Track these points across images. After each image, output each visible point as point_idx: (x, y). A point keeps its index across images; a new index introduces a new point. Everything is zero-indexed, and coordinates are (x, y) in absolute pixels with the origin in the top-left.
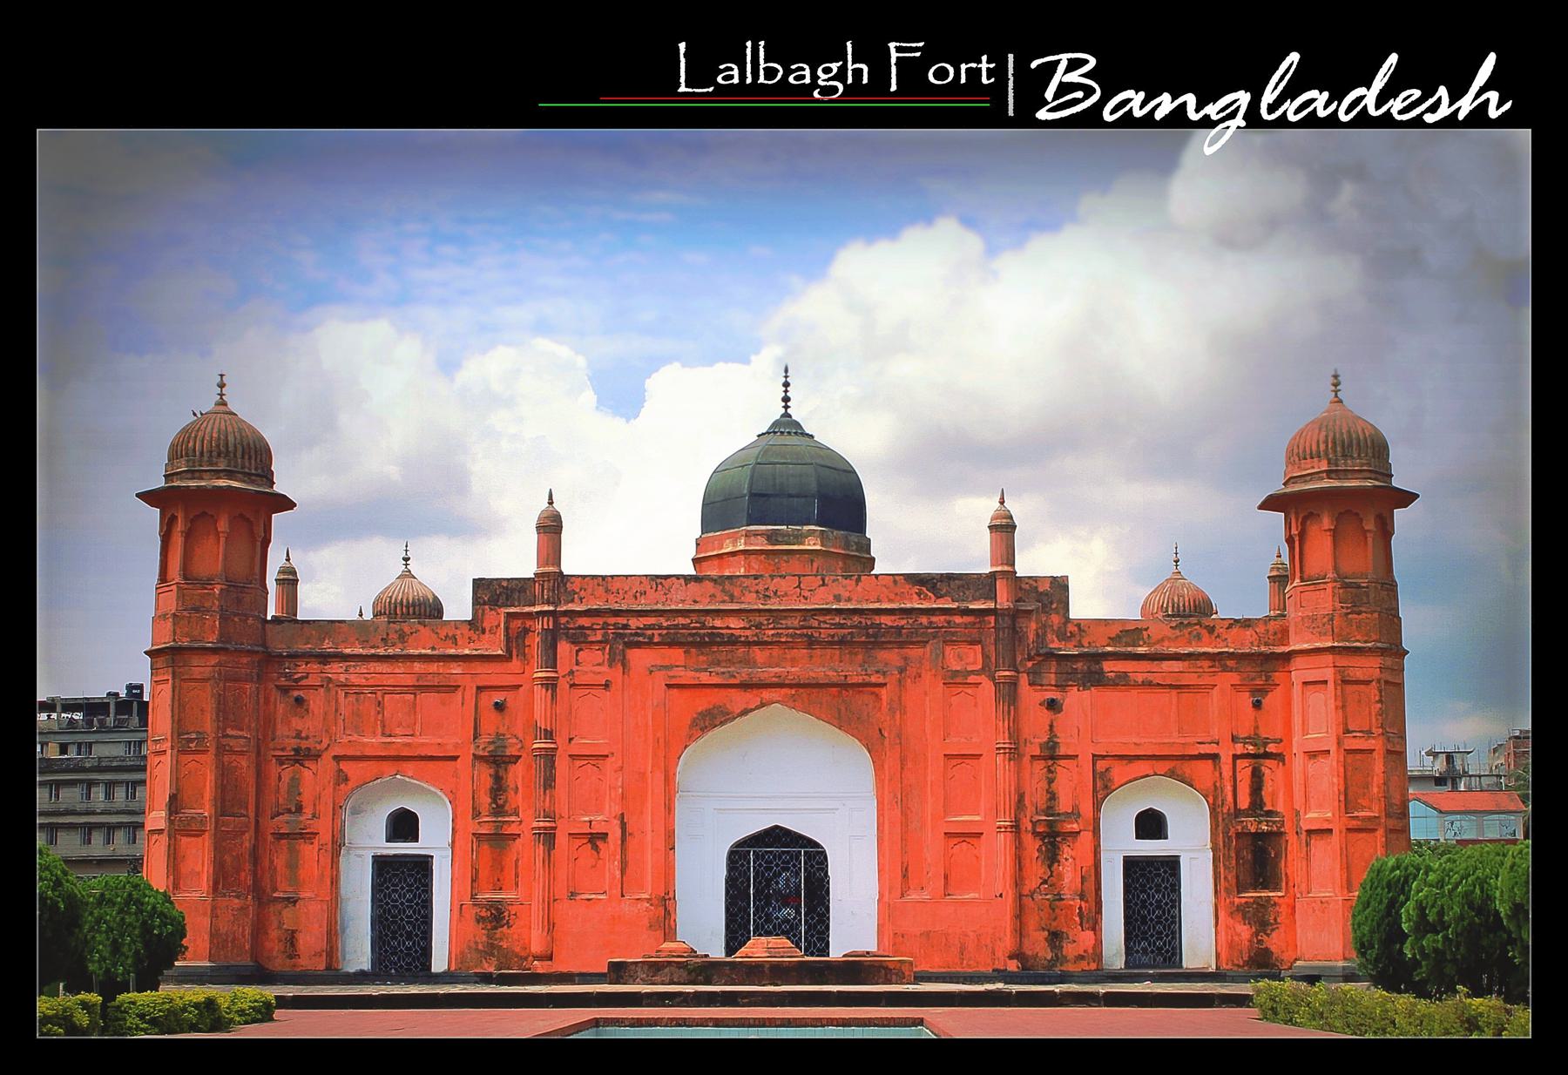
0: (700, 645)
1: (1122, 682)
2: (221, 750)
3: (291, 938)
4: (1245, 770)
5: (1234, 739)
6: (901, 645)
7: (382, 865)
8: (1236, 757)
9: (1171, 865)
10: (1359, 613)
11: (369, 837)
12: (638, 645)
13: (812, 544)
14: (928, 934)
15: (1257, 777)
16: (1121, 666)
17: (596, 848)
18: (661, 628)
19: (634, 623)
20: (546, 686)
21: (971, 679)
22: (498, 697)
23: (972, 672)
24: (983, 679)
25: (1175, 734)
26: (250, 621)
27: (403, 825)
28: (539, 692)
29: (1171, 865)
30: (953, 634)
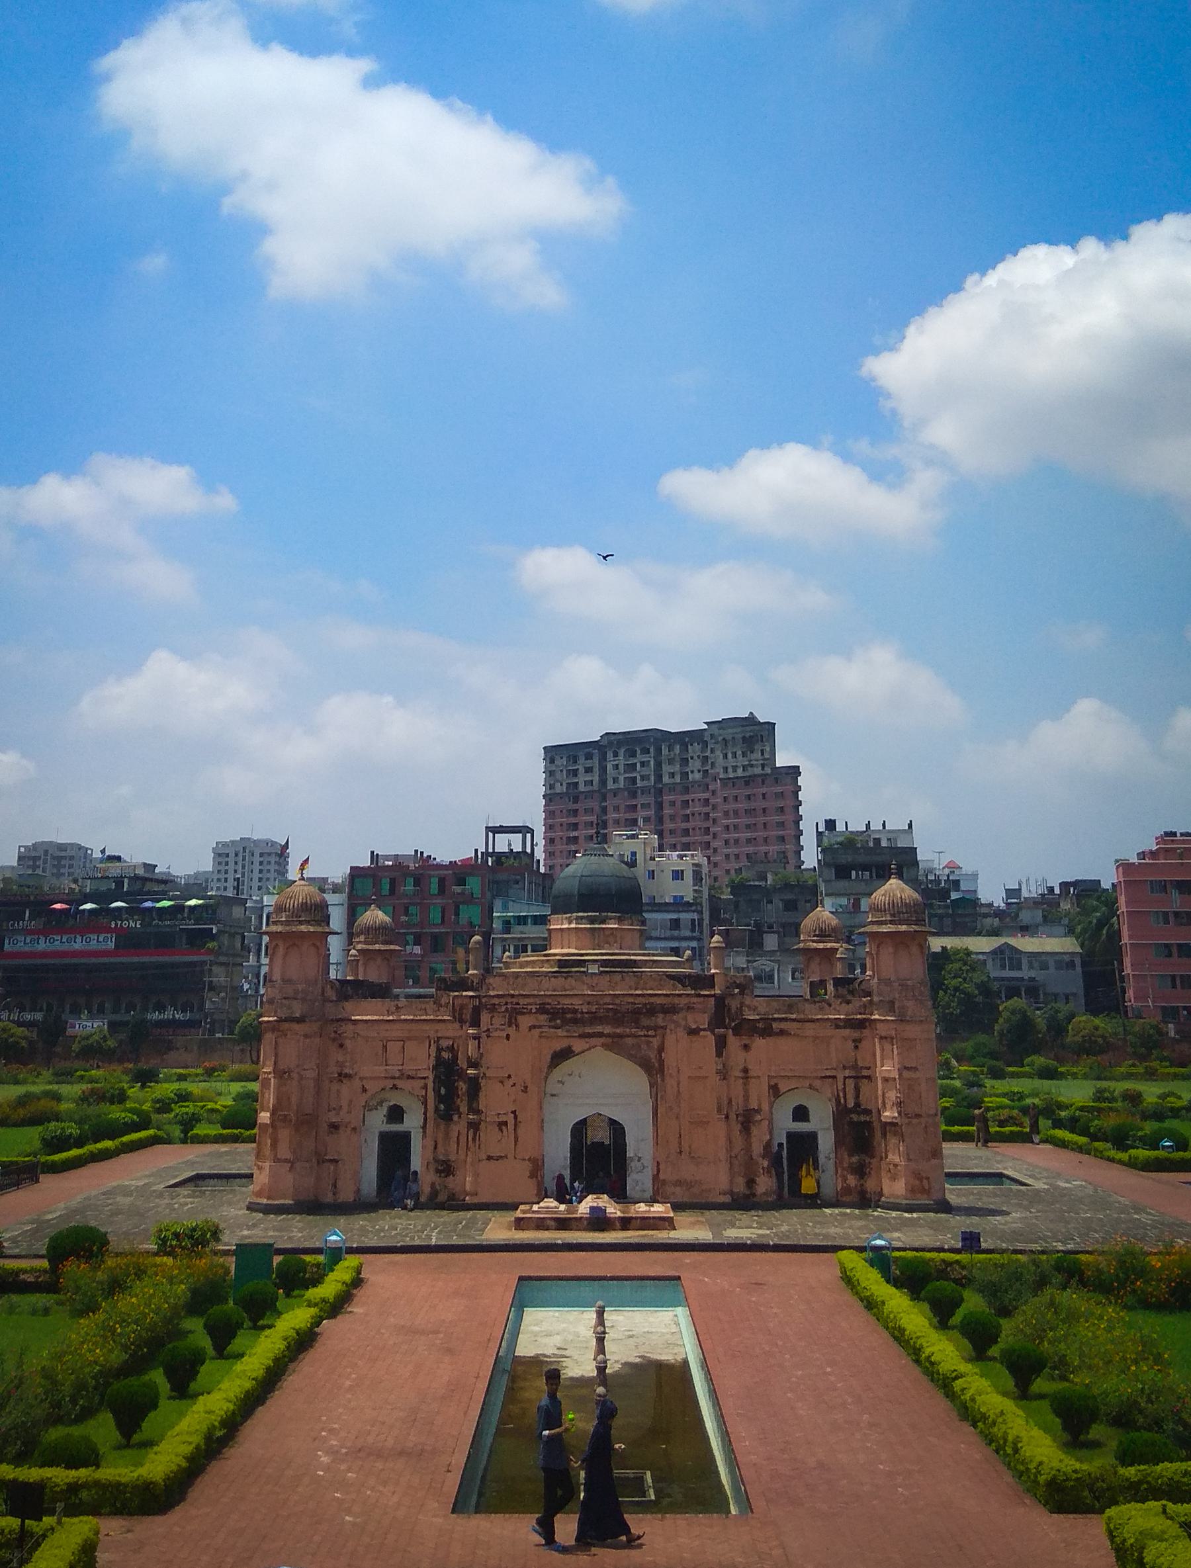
1: (782, 1033)
4: (851, 1084)
5: (845, 1068)
7: (384, 1137)
8: (845, 1078)
9: (813, 1136)
11: (377, 1122)
12: (524, 1013)
15: (857, 1089)
16: (783, 1025)
19: (521, 1001)
20: (475, 1038)
21: (702, 1033)
23: (704, 1030)
27: (396, 1114)
29: (813, 1136)
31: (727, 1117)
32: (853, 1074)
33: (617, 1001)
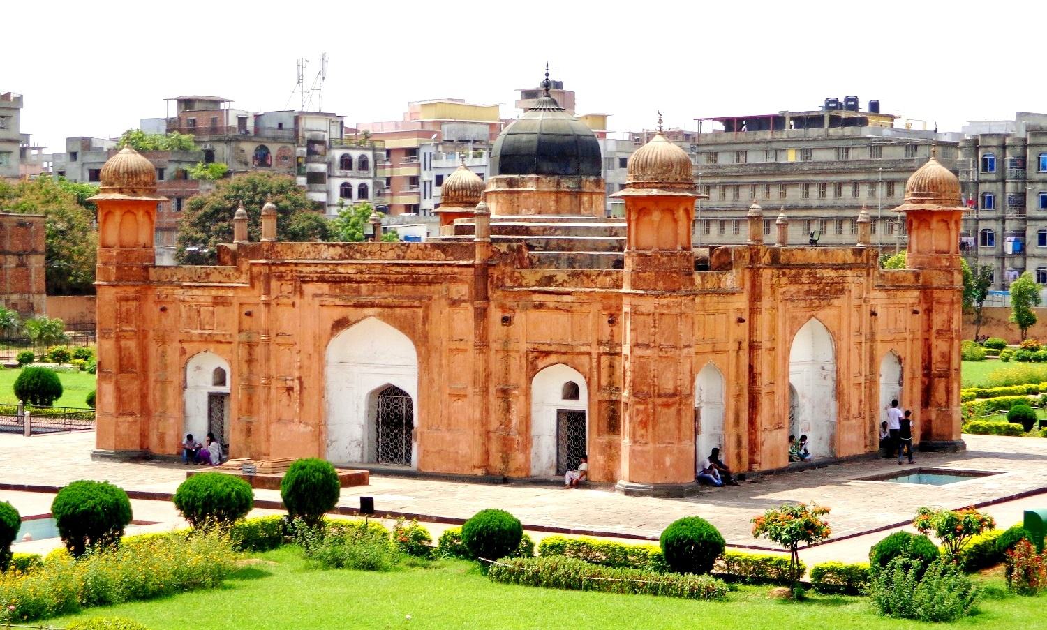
0: (335, 282)
1: (540, 306)
2: (118, 338)
3: (162, 438)
4: (605, 360)
5: (600, 343)
6: (430, 283)
8: (600, 355)
10: (645, 272)
13: (531, 187)
14: (439, 452)
15: (611, 366)
17: (289, 395)
18: (317, 273)
21: (463, 305)
22: (249, 309)
24: (468, 305)
25: (570, 340)
26: (134, 269)
28: (263, 308)
30: (454, 278)
31: (485, 392)
32: (607, 350)
33: (387, 271)
